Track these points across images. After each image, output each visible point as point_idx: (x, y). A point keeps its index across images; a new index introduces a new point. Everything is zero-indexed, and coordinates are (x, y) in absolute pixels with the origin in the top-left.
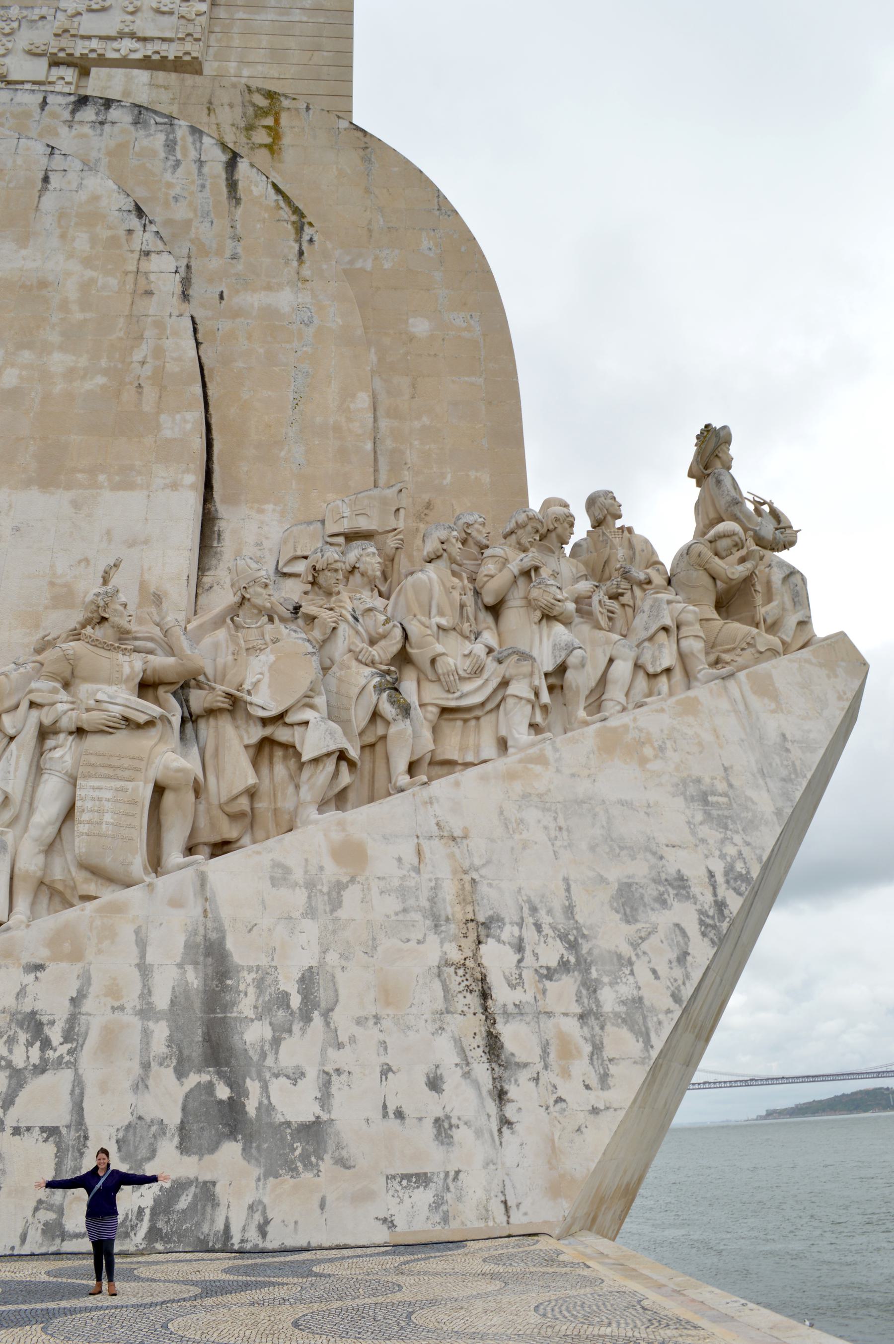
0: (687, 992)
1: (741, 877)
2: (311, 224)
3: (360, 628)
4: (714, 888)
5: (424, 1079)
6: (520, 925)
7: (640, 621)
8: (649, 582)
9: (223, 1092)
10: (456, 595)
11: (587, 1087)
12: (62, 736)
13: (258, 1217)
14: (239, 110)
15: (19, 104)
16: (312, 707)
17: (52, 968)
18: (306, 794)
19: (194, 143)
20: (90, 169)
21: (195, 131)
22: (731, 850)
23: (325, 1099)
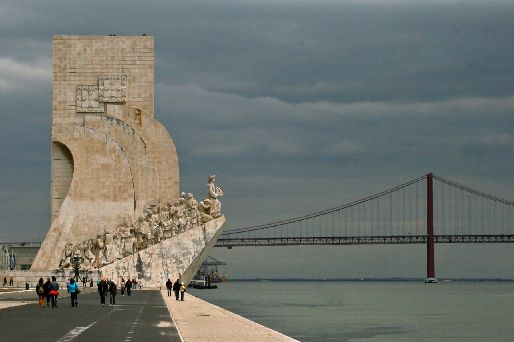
0: (189, 265)
1: (198, 252)
2: (147, 147)
3: (155, 221)
4: (195, 253)
5: (160, 273)
6: (171, 258)
7: (192, 215)
8: (195, 208)
9: (142, 274)
10: (167, 215)
11: (177, 274)
12: (123, 239)
13: (145, 285)
14: (134, 114)
15: (98, 119)
16: (149, 232)
17: (125, 263)
18: (148, 243)
19: (127, 128)
20: (113, 140)
21: (127, 125)
22: (198, 249)
23: (151, 275)
